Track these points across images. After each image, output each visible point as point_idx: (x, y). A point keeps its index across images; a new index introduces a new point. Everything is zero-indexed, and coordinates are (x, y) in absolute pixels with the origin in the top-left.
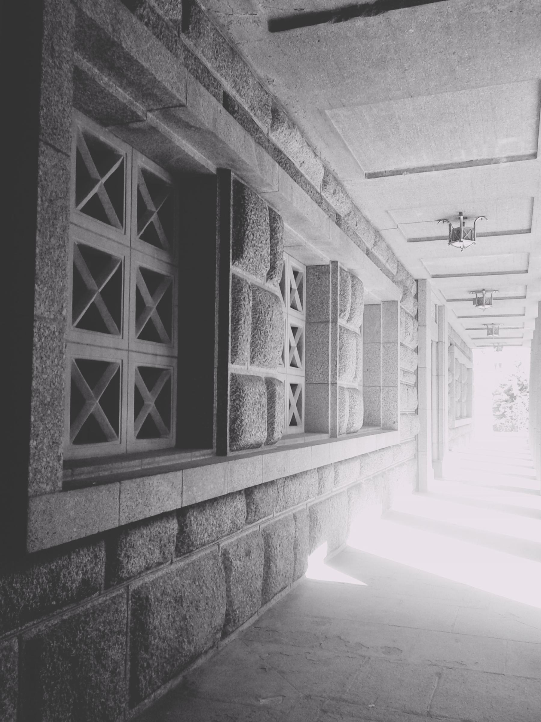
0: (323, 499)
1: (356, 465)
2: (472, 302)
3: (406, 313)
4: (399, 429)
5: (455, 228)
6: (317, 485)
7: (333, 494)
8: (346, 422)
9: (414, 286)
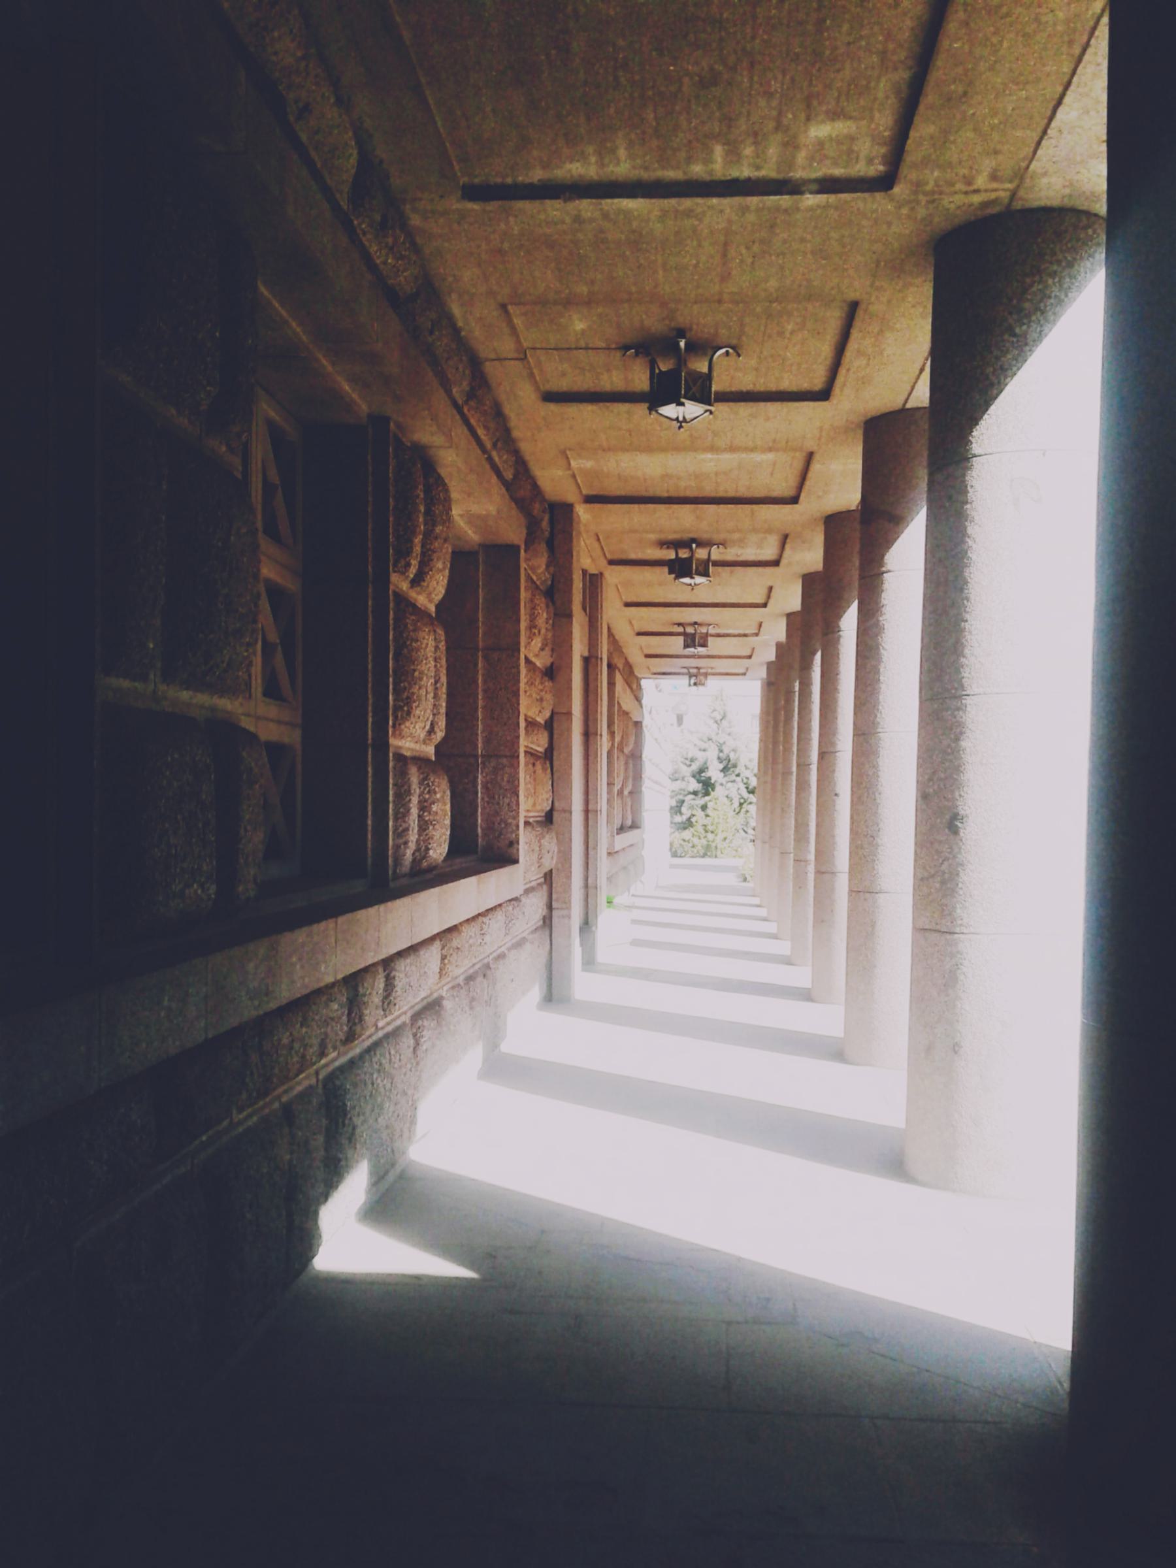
0: (358, 1051)
1: (431, 957)
2: (666, 569)
3: (533, 582)
4: (521, 859)
5: (663, 369)
6: (345, 1018)
7: (380, 1034)
8: (412, 846)
9: (547, 517)
